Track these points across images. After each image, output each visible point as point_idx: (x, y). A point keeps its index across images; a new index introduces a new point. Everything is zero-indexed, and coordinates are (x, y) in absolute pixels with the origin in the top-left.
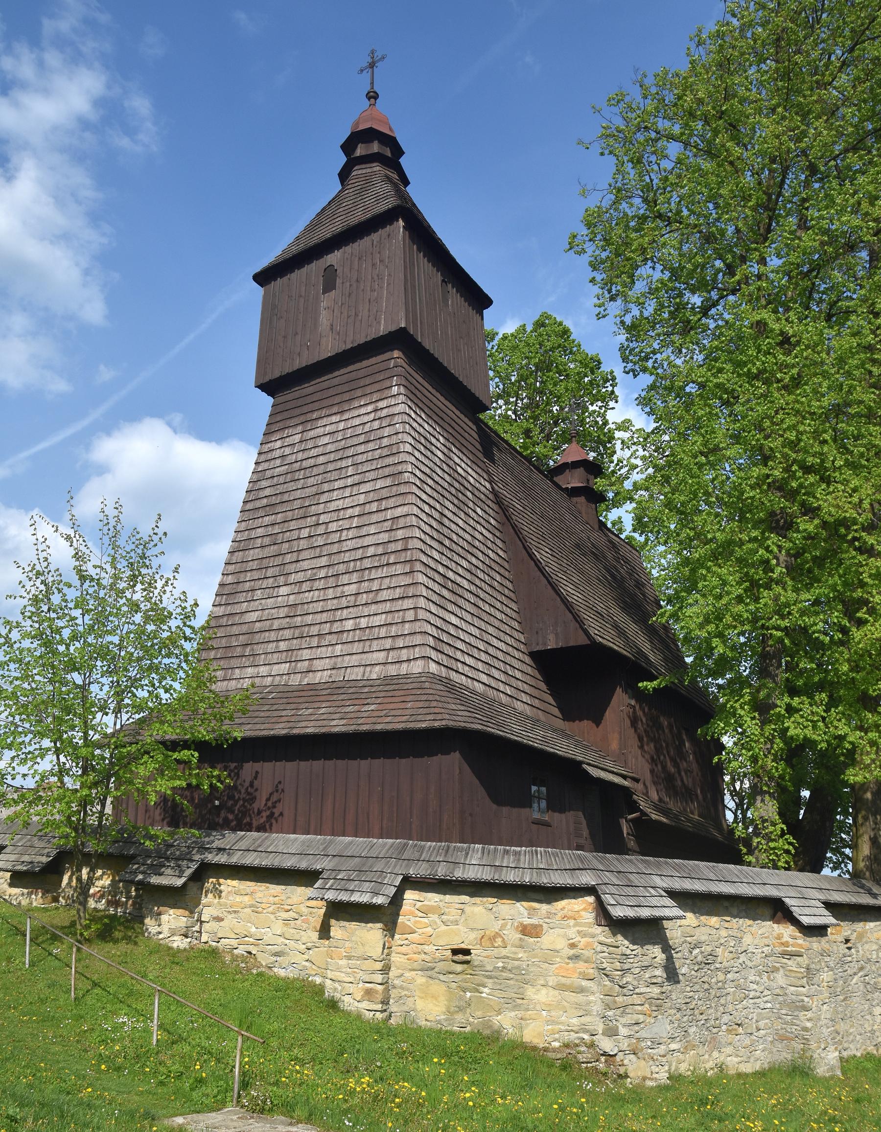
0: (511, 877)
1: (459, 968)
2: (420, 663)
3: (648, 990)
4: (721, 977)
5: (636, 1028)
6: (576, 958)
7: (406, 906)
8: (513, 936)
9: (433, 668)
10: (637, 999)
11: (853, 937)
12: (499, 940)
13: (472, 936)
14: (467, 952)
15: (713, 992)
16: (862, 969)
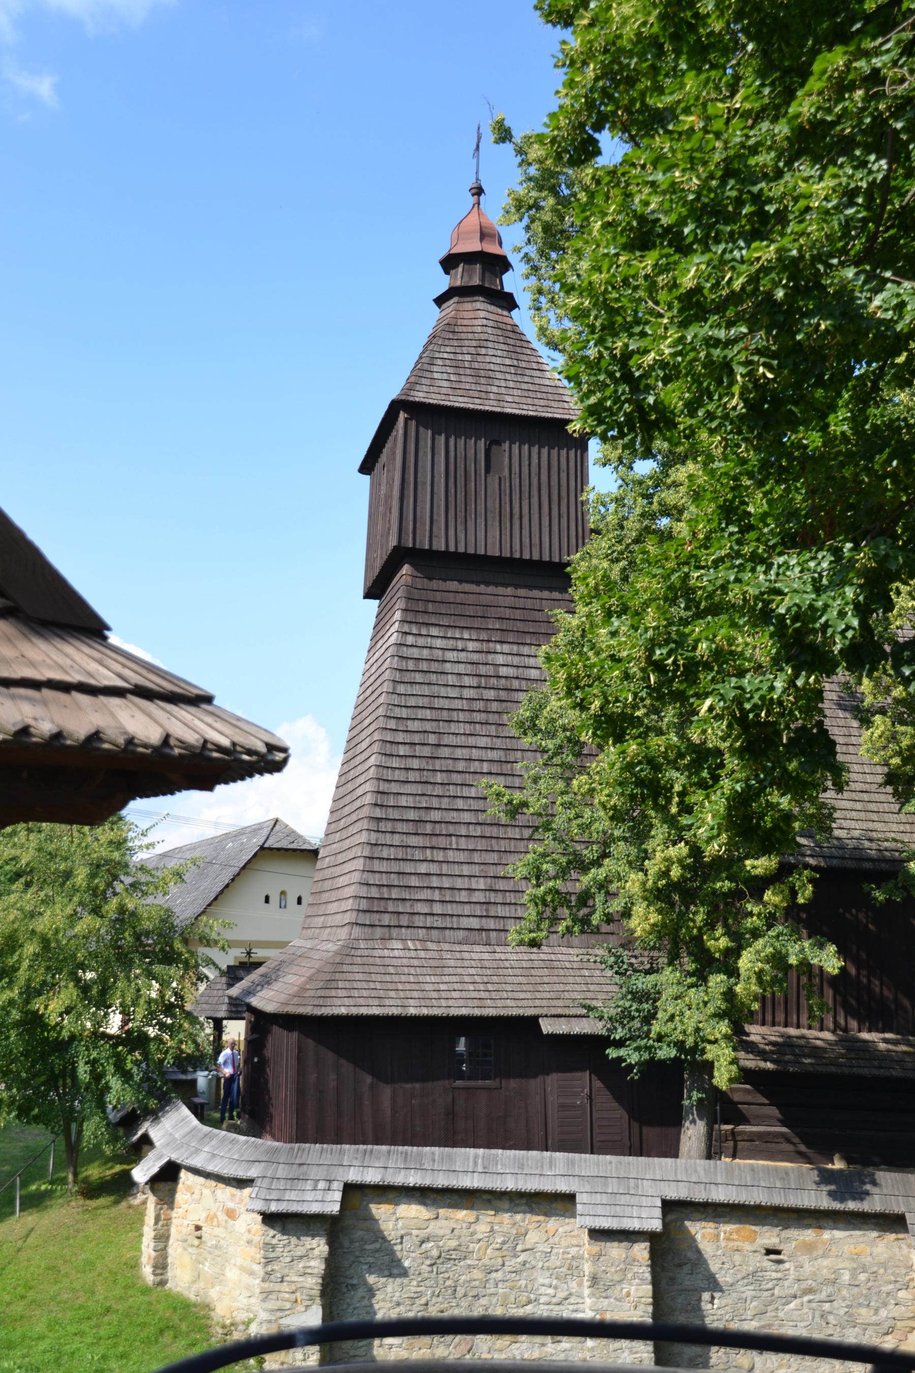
0: (210, 1168)
1: (196, 1242)
2: (346, 929)
3: (301, 1279)
4: (477, 1274)
5: (279, 1314)
6: (249, 1242)
7: (180, 1186)
8: (222, 1217)
9: (357, 931)
10: (285, 1287)
11: (787, 1248)
12: (215, 1223)
13: (204, 1215)
14: (198, 1228)
15: (461, 1291)
16: (810, 1291)
